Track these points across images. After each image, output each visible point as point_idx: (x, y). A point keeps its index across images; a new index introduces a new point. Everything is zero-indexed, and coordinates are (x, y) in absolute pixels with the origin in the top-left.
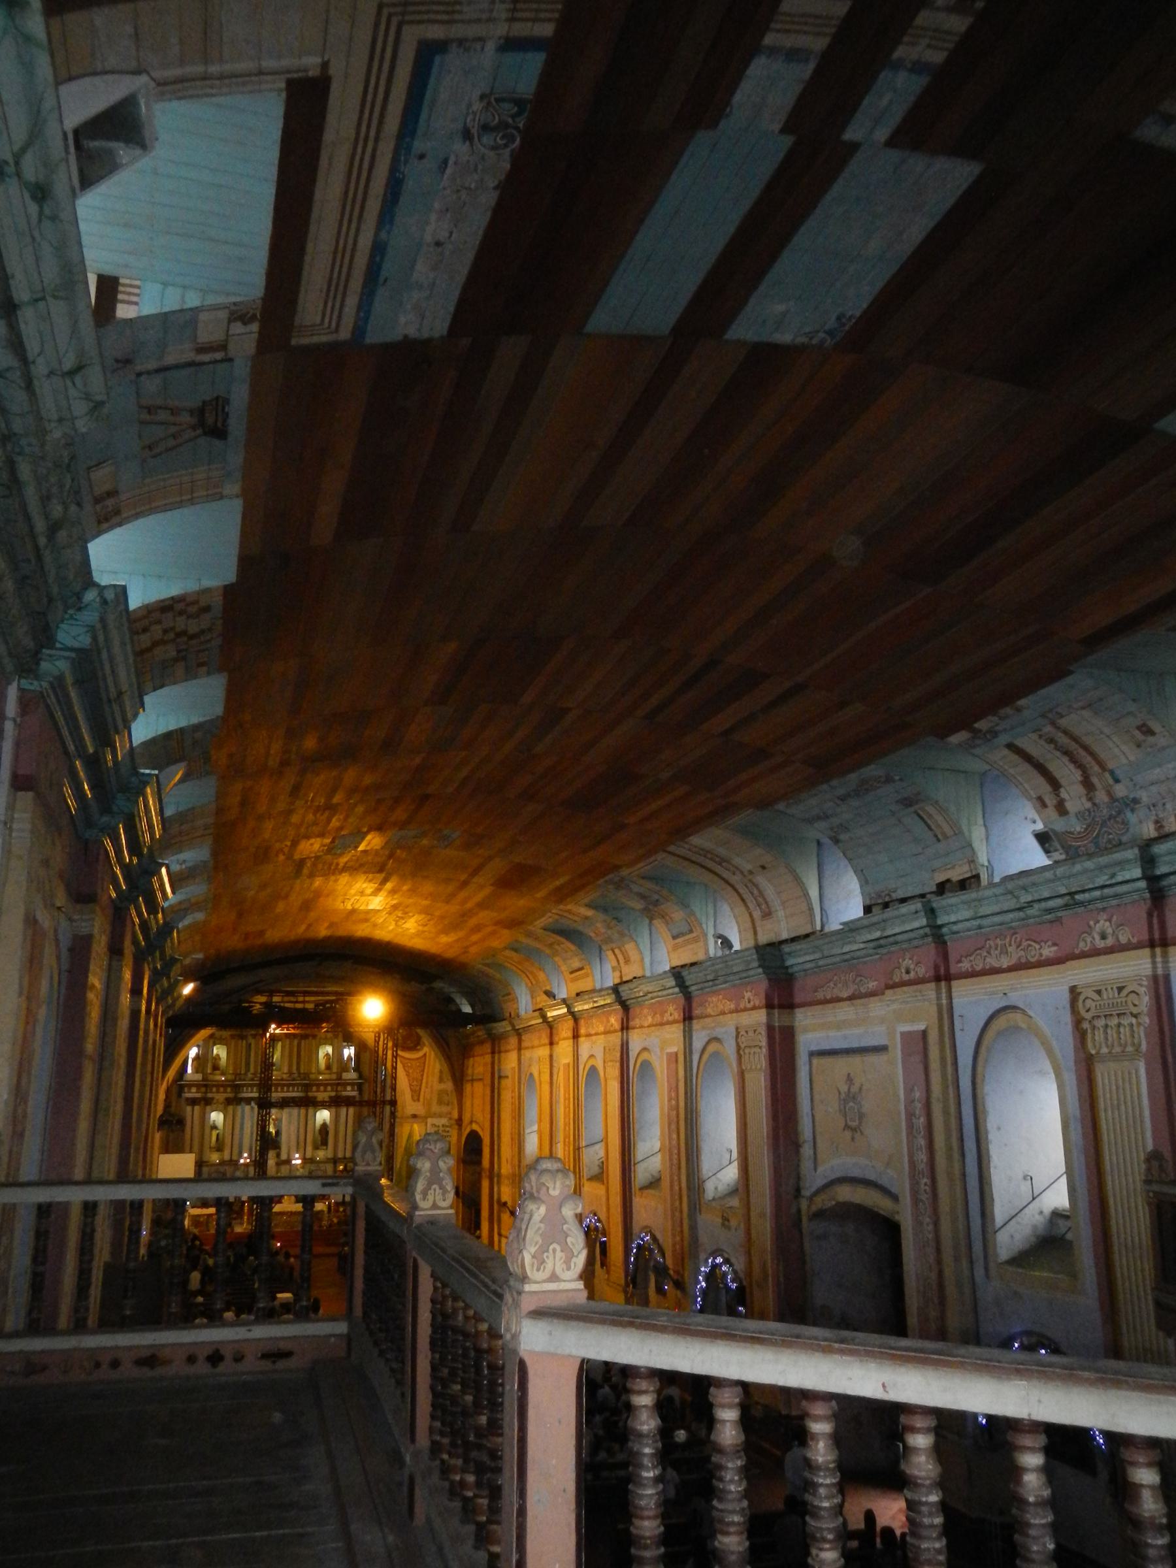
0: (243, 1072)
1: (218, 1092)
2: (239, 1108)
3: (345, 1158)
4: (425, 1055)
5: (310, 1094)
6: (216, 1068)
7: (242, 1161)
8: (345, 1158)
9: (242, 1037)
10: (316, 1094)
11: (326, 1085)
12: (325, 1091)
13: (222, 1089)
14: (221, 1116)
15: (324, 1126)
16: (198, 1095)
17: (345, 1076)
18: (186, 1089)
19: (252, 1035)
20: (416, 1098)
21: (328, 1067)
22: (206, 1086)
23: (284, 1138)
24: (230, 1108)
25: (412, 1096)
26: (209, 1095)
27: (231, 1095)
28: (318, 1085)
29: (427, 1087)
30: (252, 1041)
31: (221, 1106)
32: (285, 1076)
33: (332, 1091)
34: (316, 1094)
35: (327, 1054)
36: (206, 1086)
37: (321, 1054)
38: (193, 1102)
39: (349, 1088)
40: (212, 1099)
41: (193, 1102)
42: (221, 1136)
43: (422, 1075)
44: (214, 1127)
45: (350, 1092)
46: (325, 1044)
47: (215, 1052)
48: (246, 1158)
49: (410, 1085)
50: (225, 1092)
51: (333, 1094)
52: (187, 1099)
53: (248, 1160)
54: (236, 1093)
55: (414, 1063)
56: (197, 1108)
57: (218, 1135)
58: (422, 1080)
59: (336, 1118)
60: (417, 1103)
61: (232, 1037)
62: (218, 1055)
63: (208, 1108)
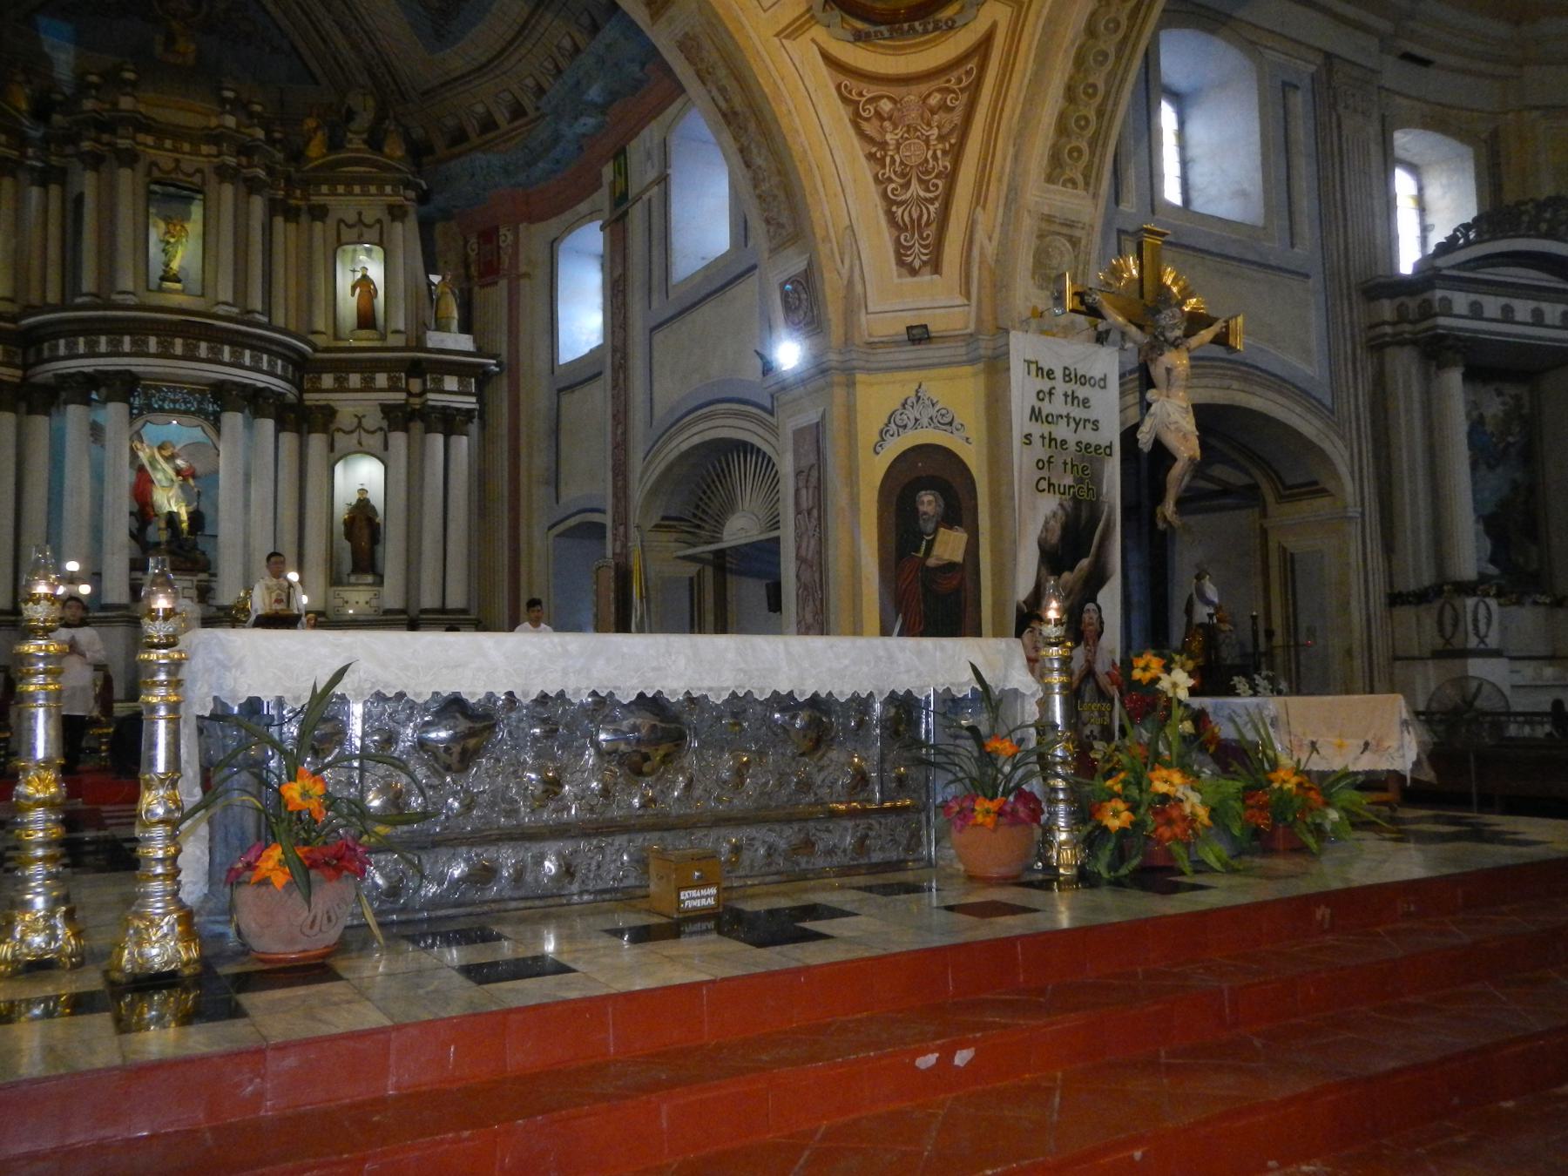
0: (53, 297)
2: (40, 425)
3: (443, 610)
4: (987, 41)
5: (311, 398)
8: (443, 610)
9: (45, 178)
10: (335, 399)
11: (369, 368)
12: (368, 387)
15: (362, 507)
17: (434, 339)
19: (81, 156)
20: (918, 256)
21: (366, 319)
23: (227, 527)
25: (900, 252)
28: (342, 368)
29: (979, 198)
30: (88, 183)
32: (221, 310)
33: (392, 389)
34: (335, 399)
35: (365, 281)
37: (345, 281)
39: (451, 383)
43: (957, 153)
45: (452, 394)
46: (360, 241)
48: (72, 579)
49: (889, 202)
51: (399, 397)
54: (26, 367)
55: (912, 95)
58: (951, 177)
59: (409, 482)
60: (926, 278)
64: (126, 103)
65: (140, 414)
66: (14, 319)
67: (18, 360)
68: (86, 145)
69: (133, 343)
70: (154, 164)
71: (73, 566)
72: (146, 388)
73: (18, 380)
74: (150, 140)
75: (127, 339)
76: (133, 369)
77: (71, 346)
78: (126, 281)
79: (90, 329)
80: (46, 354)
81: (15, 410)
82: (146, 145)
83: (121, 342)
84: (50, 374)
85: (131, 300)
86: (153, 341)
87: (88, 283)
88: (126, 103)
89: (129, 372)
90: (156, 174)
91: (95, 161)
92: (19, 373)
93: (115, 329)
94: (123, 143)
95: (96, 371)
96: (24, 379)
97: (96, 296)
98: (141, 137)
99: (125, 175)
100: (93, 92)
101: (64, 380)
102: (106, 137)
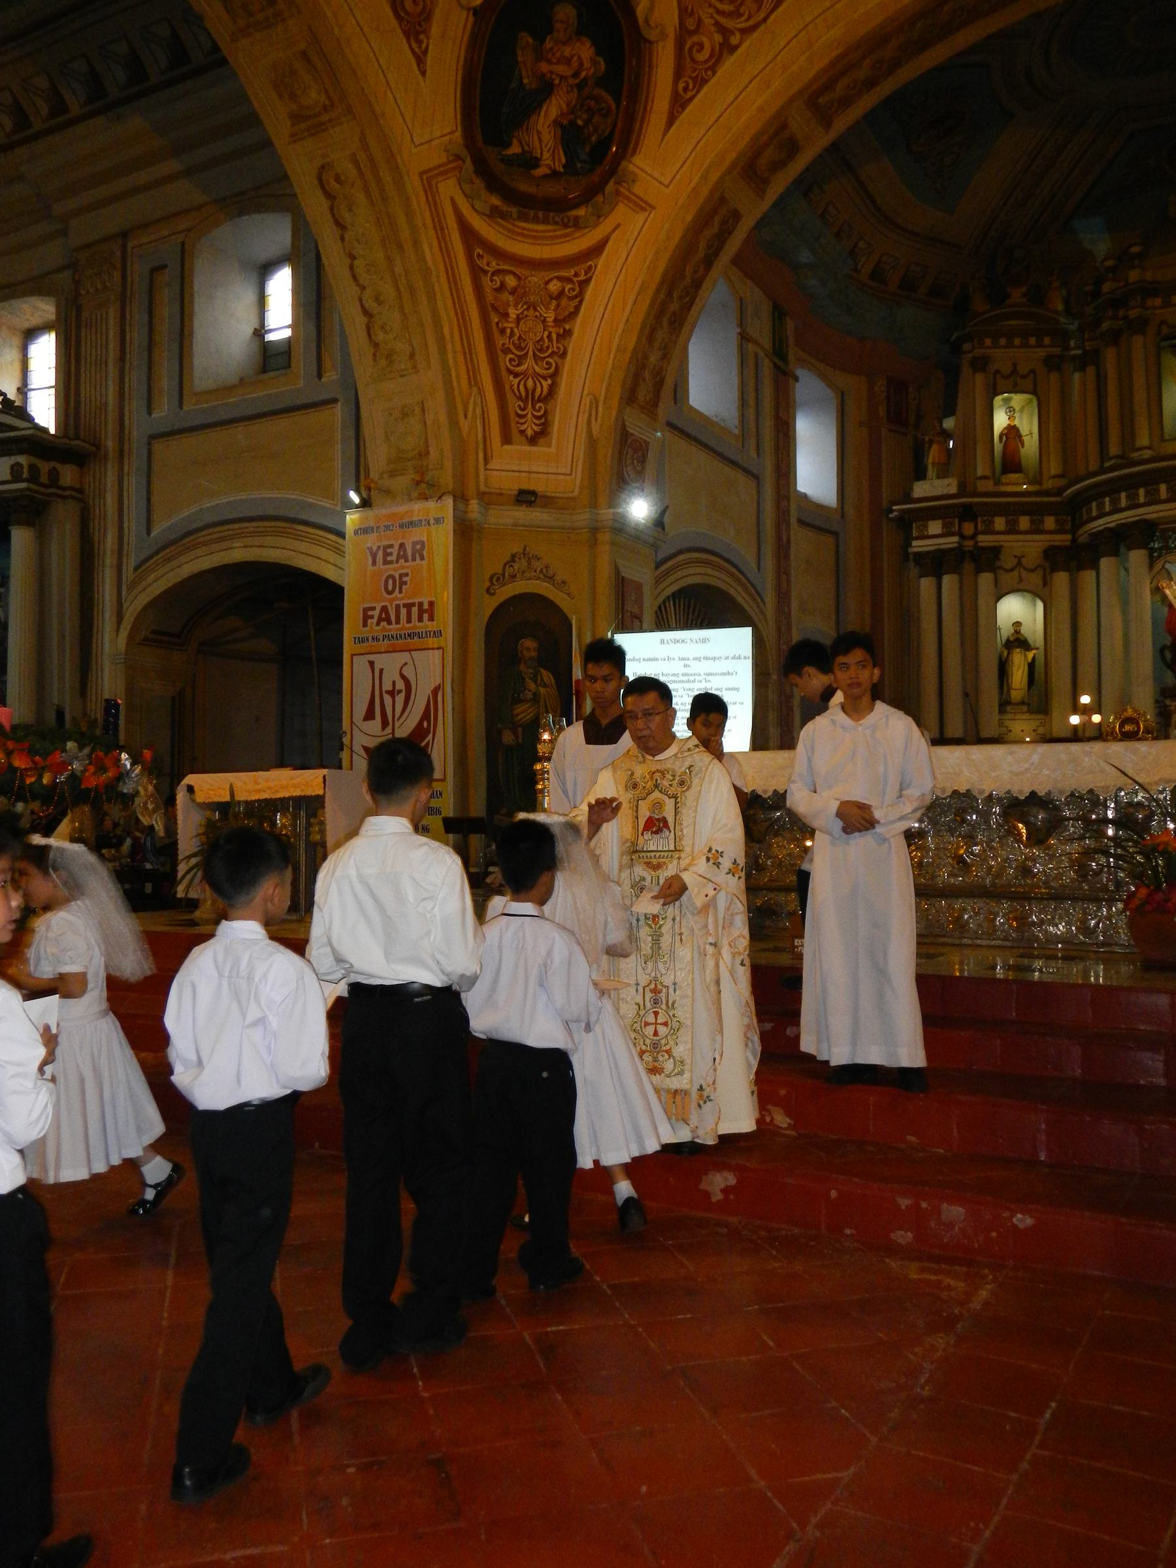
1: (1012, 529)
2: (1088, 576)
6: (1011, 464)
7: (1075, 720)
9: (1082, 363)
13: (1024, 522)
14: (1040, 606)
16: (952, 541)
18: (915, 533)
22: (968, 513)
24: (1061, 579)
26: (985, 540)
27: (1064, 539)
31: (1036, 579)
36: (968, 513)
38: (936, 564)
40: (996, 551)
41: (936, 564)
42: (1040, 661)
44: (1018, 641)
47: (1001, 420)
48: (1086, 711)
50: (1036, 529)
52: (919, 556)
53: (1096, 718)
56: (949, 581)
57: (1032, 666)
61: (1053, 364)
62: (1012, 432)
63: (986, 579)
64: (1134, 275)
65: (1159, 557)
66: (1059, 492)
67: (1068, 527)
68: (1106, 325)
69: (1147, 494)
70: (1162, 322)
71: (1085, 699)
72: (1165, 530)
73: (1068, 543)
74: (1158, 301)
75: (1141, 491)
76: (1147, 517)
77: (1101, 507)
78: (1143, 439)
79: (1111, 489)
80: (1085, 517)
81: (1068, 570)
82: (1156, 308)
83: (1136, 495)
84: (1086, 535)
85: (1147, 454)
86: (1163, 488)
87: (1114, 450)
88: (1134, 275)
89: (1146, 521)
90: (1165, 331)
91: (1114, 337)
92: (1069, 537)
93: (1130, 484)
94: (1133, 313)
95: (1118, 525)
96: (1074, 540)
97: (1122, 457)
98: (1150, 302)
99: (1138, 342)
100: (1110, 275)
101: (1096, 535)
102: (1121, 313)
